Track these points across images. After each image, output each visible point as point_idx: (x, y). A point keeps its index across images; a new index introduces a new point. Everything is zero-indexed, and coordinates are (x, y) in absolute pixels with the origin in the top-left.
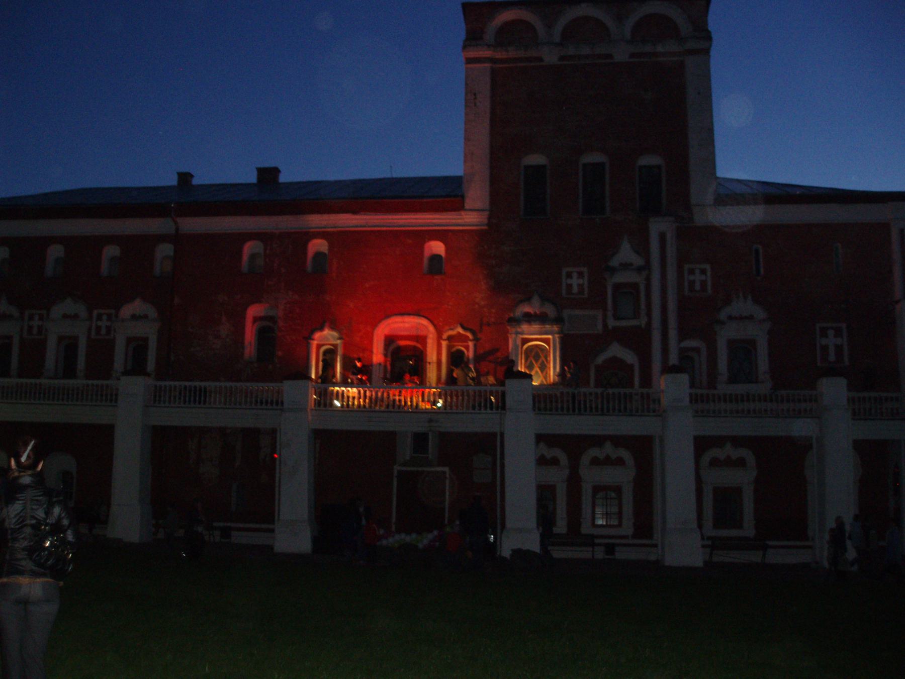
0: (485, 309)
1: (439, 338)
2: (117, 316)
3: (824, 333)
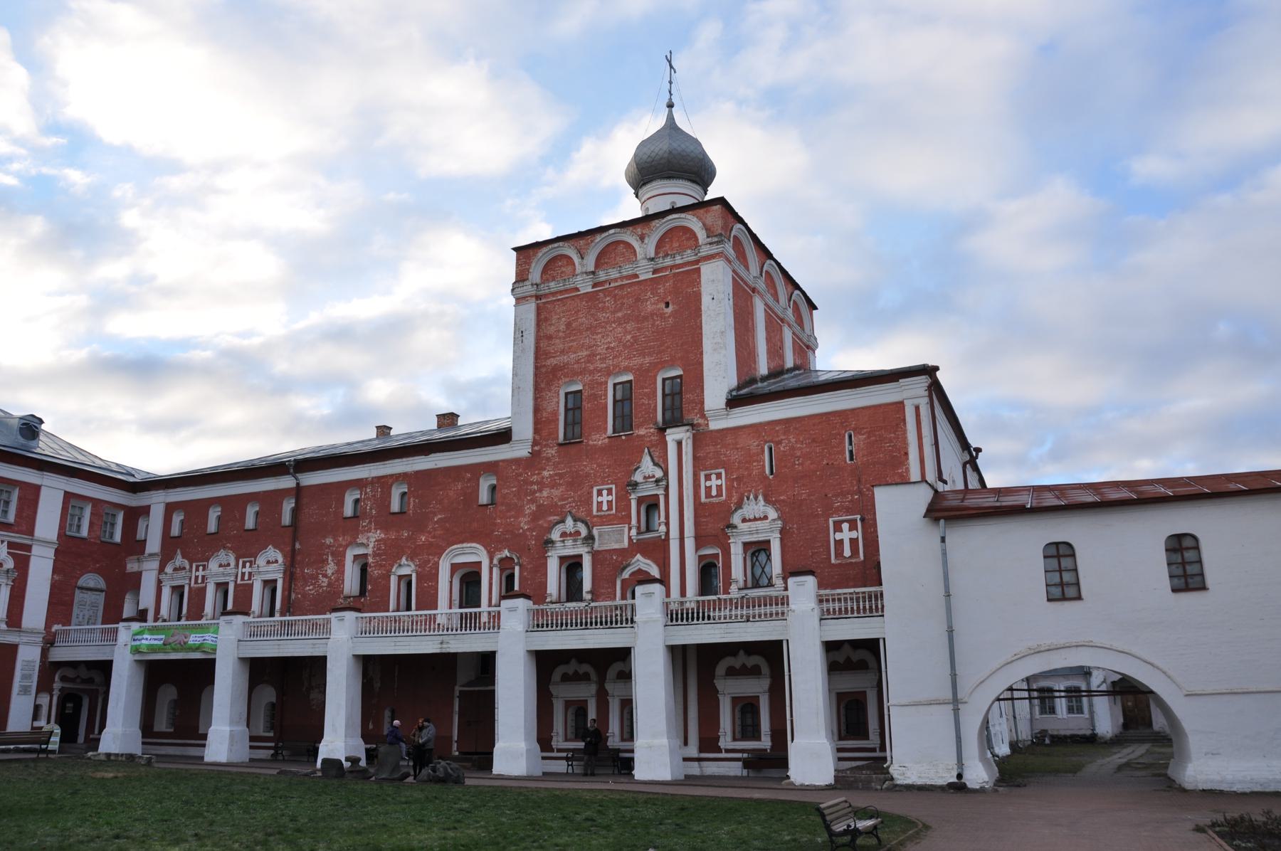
0: (528, 533)
2: (255, 564)
3: (838, 528)
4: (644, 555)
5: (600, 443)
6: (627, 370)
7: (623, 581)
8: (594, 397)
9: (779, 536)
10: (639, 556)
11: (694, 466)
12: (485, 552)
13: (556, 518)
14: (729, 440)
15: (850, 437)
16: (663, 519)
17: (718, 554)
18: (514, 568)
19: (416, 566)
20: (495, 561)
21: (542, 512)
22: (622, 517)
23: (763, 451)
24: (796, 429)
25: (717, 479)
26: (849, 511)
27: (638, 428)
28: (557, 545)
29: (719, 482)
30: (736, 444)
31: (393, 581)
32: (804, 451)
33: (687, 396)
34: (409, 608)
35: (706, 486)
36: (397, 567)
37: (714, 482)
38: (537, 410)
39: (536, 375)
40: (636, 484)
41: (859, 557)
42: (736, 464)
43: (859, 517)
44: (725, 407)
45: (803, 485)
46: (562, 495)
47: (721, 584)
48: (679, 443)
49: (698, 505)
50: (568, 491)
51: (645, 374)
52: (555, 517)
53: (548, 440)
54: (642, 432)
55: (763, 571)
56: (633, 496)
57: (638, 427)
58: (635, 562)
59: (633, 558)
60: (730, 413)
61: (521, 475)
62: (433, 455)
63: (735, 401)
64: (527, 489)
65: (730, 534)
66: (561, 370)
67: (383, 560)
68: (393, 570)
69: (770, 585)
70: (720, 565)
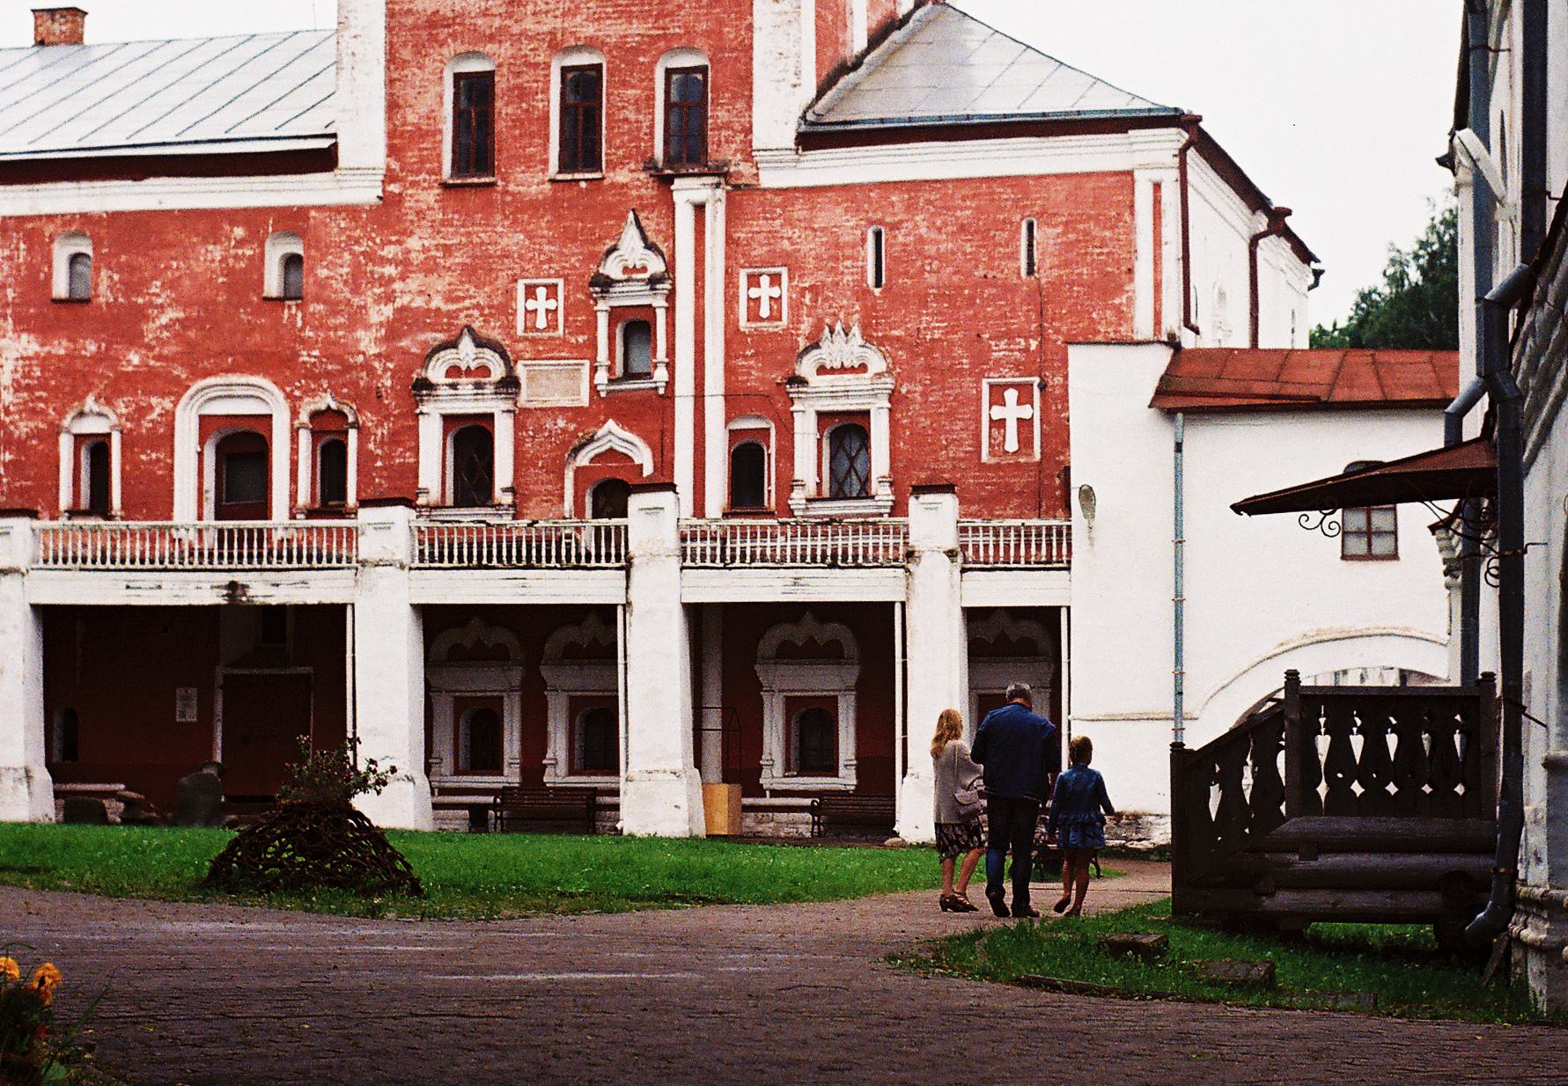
0: (376, 364)
1: (295, 413)
3: (997, 397)
4: (625, 421)
5: (534, 189)
6: (590, 45)
7: (578, 471)
8: (522, 93)
9: (889, 405)
10: (611, 425)
11: (727, 257)
12: (280, 395)
13: (441, 337)
14: (799, 211)
15: (1030, 226)
16: (661, 354)
17: (768, 430)
18: (346, 433)
19: (120, 416)
20: (304, 417)
21: (404, 322)
22: (577, 346)
23: (864, 240)
24: (929, 202)
25: (772, 284)
26: (1017, 367)
27: (614, 169)
28: (439, 392)
29: (775, 292)
30: (811, 220)
31: (66, 445)
32: (943, 247)
33: (718, 114)
34: (100, 505)
35: (749, 299)
36: (73, 418)
37: (765, 291)
38: (393, 106)
39: (389, 29)
40: (605, 284)
41: (1031, 455)
42: (811, 260)
43: (1036, 380)
44: (793, 147)
45: (940, 313)
46: (451, 291)
47: (773, 488)
48: (699, 208)
49: (733, 337)
50: (462, 283)
51: (630, 56)
52: (434, 335)
53: (418, 172)
54: (622, 176)
55: (852, 466)
56: (602, 306)
57: (612, 166)
58: (604, 436)
59: (600, 427)
60: (802, 158)
61: (357, 242)
62: (152, 181)
63: (813, 138)
64: (372, 273)
65: (794, 395)
66: (448, 26)
67: (40, 399)
68: (66, 423)
69: (865, 494)
70: (773, 450)
